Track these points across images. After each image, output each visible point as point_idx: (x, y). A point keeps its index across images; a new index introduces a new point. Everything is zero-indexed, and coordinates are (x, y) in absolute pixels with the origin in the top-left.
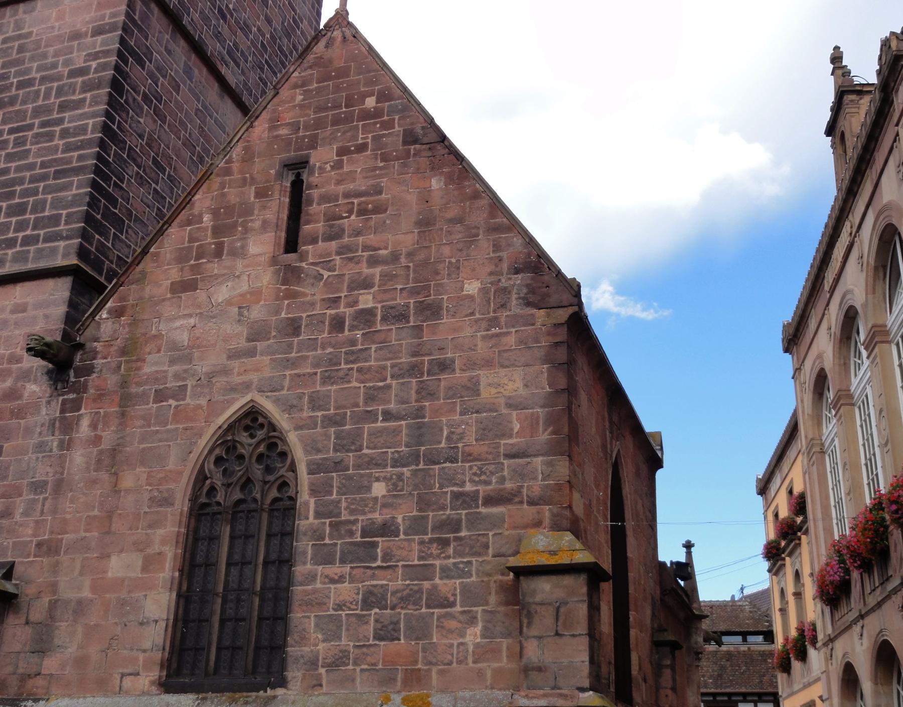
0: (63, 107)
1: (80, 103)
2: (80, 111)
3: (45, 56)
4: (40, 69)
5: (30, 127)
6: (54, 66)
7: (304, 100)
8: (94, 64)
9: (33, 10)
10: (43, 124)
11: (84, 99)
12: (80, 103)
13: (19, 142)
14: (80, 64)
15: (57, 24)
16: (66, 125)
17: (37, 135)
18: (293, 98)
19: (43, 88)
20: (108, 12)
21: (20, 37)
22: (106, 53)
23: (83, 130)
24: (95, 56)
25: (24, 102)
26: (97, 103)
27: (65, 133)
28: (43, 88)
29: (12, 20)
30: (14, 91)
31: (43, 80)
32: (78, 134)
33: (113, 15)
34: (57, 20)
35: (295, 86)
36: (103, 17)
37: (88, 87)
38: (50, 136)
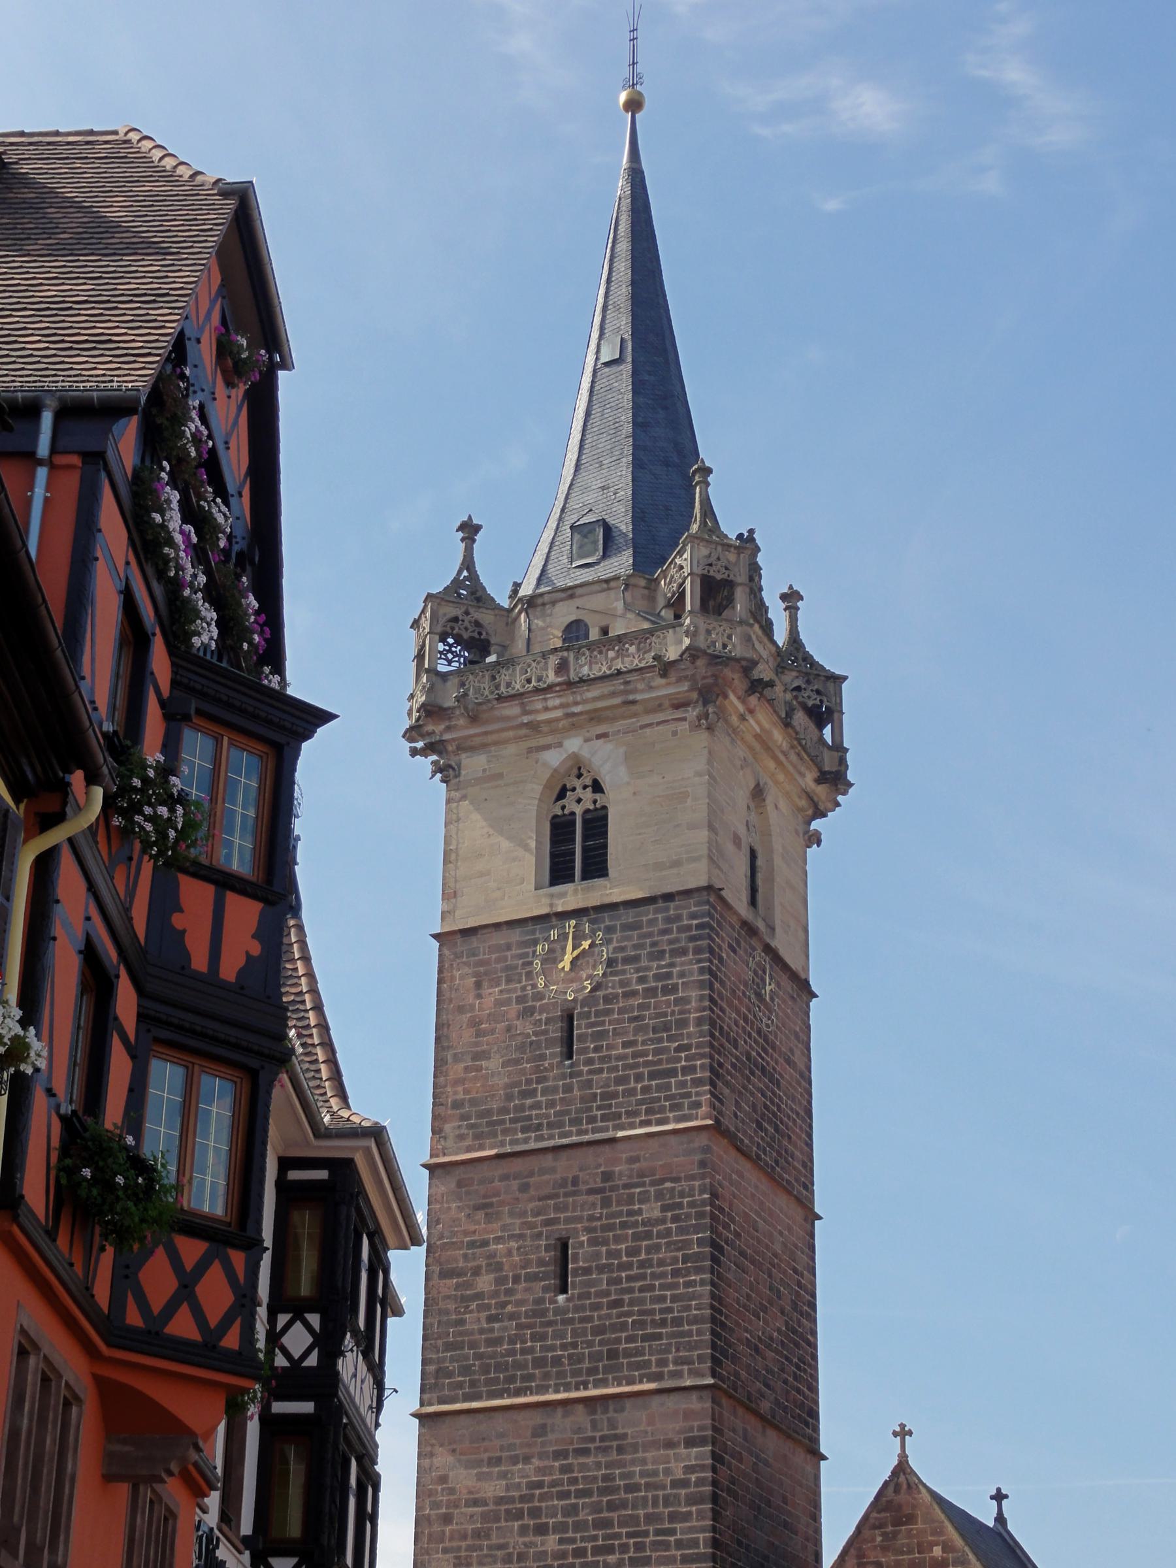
0: (673, 1517)
1: (687, 1517)
2: (688, 1524)
3: (644, 1462)
4: (643, 1474)
5: (646, 1534)
6: (655, 1473)
7: (882, 1541)
8: (693, 1478)
9: (622, 1410)
10: (658, 1532)
11: (690, 1513)
12: (687, 1517)
13: (639, 1547)
14: (680, 1475)
15: (649, 1429)
16: (679, 1536)
17: (654, 1543)
18: (874, 1540)
19: (650, 1495)
20: (696, 1424)
21: (616, 1437)
22: (702, 1468)
23: (695, 1543)
24: (689, 1469)
25: (634, 1507)
26: (703, 1519)
27: (679, 1544)
28: (650, 1495)
29: (604, 1417)
30: (623, 1495)
31: (648, 1486)
32: (690, 1548)
33: (701, 1428)
34: (649, 1424)
35: (874, 1527)
36: (691, 1429)
37: (692, 1500)
38: (666, 1546)
